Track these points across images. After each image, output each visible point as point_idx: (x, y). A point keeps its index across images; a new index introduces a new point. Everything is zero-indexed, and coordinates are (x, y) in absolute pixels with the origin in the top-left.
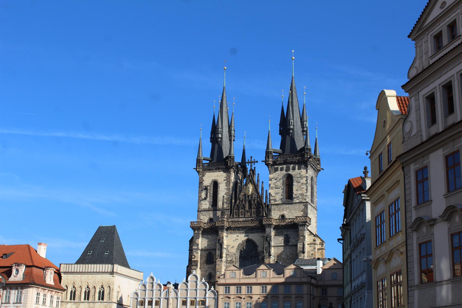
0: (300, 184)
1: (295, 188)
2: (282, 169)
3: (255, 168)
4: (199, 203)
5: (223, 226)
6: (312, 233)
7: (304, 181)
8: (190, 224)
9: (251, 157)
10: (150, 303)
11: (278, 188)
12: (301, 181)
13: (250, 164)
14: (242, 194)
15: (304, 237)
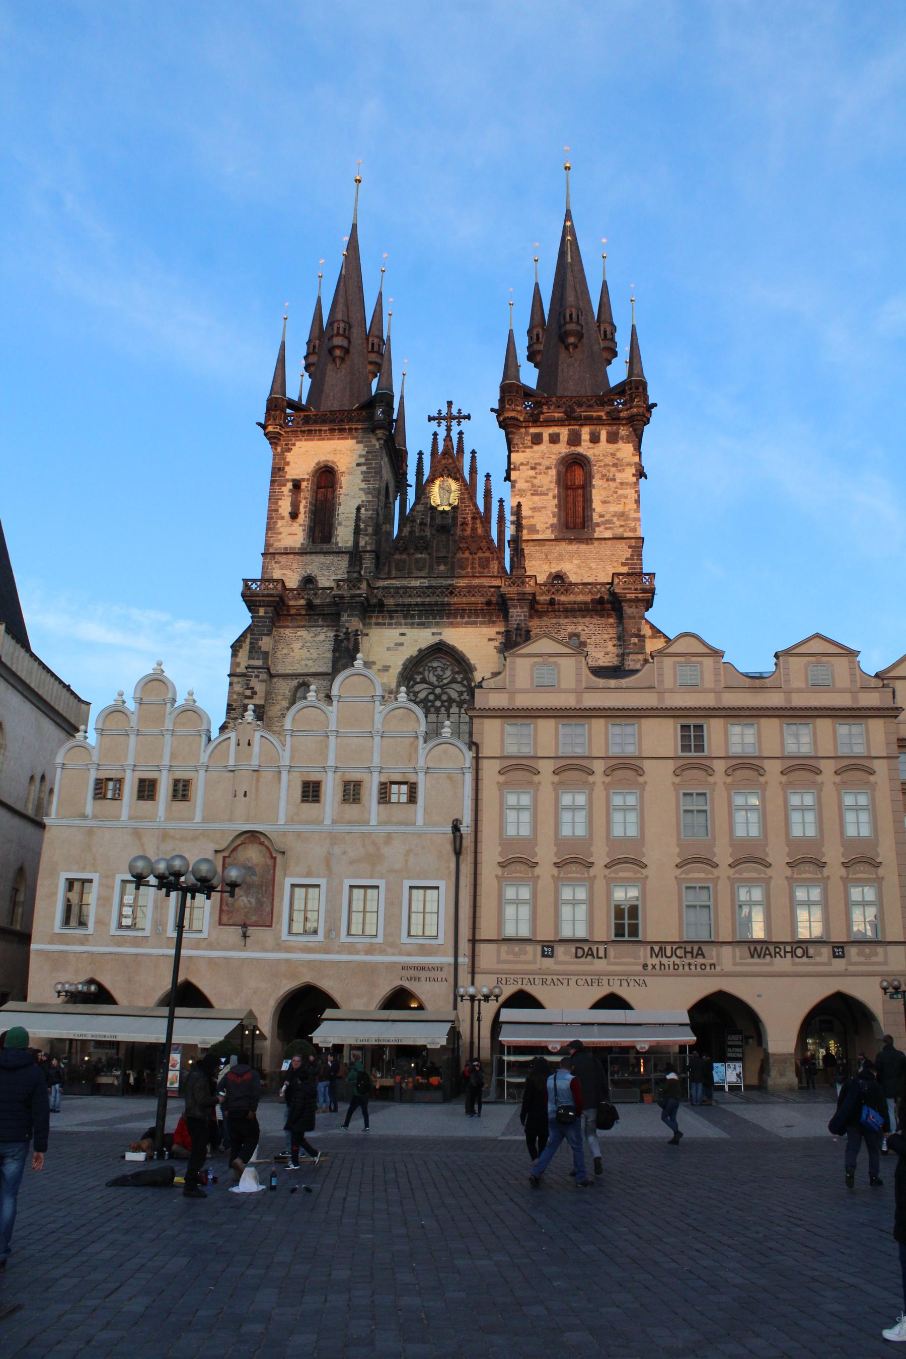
0: (612, 484)
1: (597, 496)
2: (554, 439)
3: (461, 433)
4: (268, 529)
5: (360, 595)
6: (659, 632)
7: (628, 475)
8: (240, 587)
9: (450, 404)
10: (147, 789)
11: (542, 494)
12: (620, 477)
13: (444, 423)
14: (420, 508)
15: (642, 638)
